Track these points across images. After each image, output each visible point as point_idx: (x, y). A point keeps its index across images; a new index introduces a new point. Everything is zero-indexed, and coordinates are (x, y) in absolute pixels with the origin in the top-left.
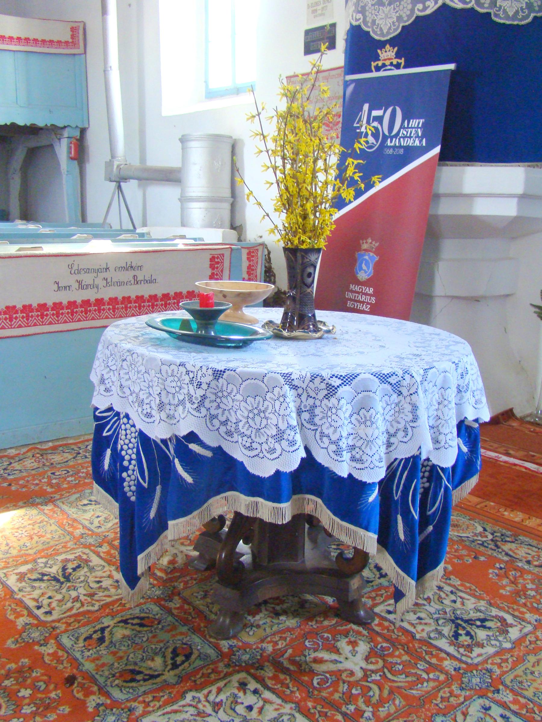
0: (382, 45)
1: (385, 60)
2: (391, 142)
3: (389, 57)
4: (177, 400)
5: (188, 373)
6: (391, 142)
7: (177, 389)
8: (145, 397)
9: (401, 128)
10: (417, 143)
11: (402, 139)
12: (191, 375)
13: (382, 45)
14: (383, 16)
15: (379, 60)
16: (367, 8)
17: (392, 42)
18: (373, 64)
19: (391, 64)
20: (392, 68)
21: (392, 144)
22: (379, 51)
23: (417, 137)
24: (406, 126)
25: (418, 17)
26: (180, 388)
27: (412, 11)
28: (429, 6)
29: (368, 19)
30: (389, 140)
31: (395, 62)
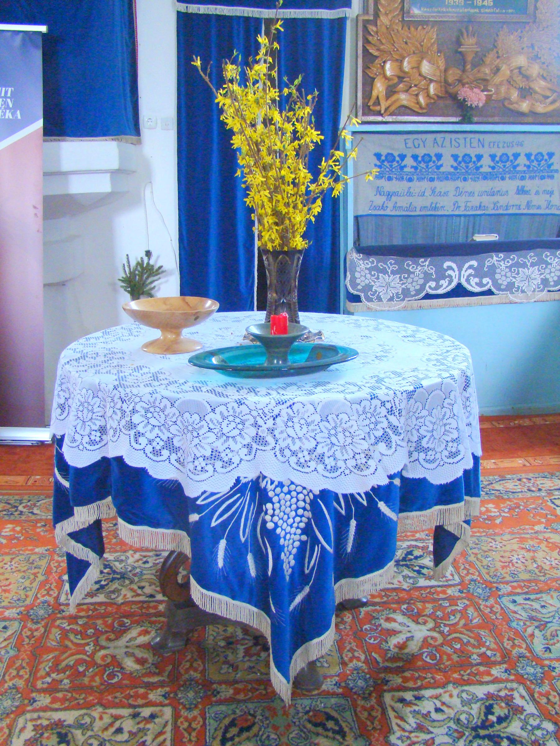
4: (373, 438)
5: (383, 404)
7: (372, 426)
8: (325, 450)
10: (9, 115)
12: (388, 405)
26: (376, 424)
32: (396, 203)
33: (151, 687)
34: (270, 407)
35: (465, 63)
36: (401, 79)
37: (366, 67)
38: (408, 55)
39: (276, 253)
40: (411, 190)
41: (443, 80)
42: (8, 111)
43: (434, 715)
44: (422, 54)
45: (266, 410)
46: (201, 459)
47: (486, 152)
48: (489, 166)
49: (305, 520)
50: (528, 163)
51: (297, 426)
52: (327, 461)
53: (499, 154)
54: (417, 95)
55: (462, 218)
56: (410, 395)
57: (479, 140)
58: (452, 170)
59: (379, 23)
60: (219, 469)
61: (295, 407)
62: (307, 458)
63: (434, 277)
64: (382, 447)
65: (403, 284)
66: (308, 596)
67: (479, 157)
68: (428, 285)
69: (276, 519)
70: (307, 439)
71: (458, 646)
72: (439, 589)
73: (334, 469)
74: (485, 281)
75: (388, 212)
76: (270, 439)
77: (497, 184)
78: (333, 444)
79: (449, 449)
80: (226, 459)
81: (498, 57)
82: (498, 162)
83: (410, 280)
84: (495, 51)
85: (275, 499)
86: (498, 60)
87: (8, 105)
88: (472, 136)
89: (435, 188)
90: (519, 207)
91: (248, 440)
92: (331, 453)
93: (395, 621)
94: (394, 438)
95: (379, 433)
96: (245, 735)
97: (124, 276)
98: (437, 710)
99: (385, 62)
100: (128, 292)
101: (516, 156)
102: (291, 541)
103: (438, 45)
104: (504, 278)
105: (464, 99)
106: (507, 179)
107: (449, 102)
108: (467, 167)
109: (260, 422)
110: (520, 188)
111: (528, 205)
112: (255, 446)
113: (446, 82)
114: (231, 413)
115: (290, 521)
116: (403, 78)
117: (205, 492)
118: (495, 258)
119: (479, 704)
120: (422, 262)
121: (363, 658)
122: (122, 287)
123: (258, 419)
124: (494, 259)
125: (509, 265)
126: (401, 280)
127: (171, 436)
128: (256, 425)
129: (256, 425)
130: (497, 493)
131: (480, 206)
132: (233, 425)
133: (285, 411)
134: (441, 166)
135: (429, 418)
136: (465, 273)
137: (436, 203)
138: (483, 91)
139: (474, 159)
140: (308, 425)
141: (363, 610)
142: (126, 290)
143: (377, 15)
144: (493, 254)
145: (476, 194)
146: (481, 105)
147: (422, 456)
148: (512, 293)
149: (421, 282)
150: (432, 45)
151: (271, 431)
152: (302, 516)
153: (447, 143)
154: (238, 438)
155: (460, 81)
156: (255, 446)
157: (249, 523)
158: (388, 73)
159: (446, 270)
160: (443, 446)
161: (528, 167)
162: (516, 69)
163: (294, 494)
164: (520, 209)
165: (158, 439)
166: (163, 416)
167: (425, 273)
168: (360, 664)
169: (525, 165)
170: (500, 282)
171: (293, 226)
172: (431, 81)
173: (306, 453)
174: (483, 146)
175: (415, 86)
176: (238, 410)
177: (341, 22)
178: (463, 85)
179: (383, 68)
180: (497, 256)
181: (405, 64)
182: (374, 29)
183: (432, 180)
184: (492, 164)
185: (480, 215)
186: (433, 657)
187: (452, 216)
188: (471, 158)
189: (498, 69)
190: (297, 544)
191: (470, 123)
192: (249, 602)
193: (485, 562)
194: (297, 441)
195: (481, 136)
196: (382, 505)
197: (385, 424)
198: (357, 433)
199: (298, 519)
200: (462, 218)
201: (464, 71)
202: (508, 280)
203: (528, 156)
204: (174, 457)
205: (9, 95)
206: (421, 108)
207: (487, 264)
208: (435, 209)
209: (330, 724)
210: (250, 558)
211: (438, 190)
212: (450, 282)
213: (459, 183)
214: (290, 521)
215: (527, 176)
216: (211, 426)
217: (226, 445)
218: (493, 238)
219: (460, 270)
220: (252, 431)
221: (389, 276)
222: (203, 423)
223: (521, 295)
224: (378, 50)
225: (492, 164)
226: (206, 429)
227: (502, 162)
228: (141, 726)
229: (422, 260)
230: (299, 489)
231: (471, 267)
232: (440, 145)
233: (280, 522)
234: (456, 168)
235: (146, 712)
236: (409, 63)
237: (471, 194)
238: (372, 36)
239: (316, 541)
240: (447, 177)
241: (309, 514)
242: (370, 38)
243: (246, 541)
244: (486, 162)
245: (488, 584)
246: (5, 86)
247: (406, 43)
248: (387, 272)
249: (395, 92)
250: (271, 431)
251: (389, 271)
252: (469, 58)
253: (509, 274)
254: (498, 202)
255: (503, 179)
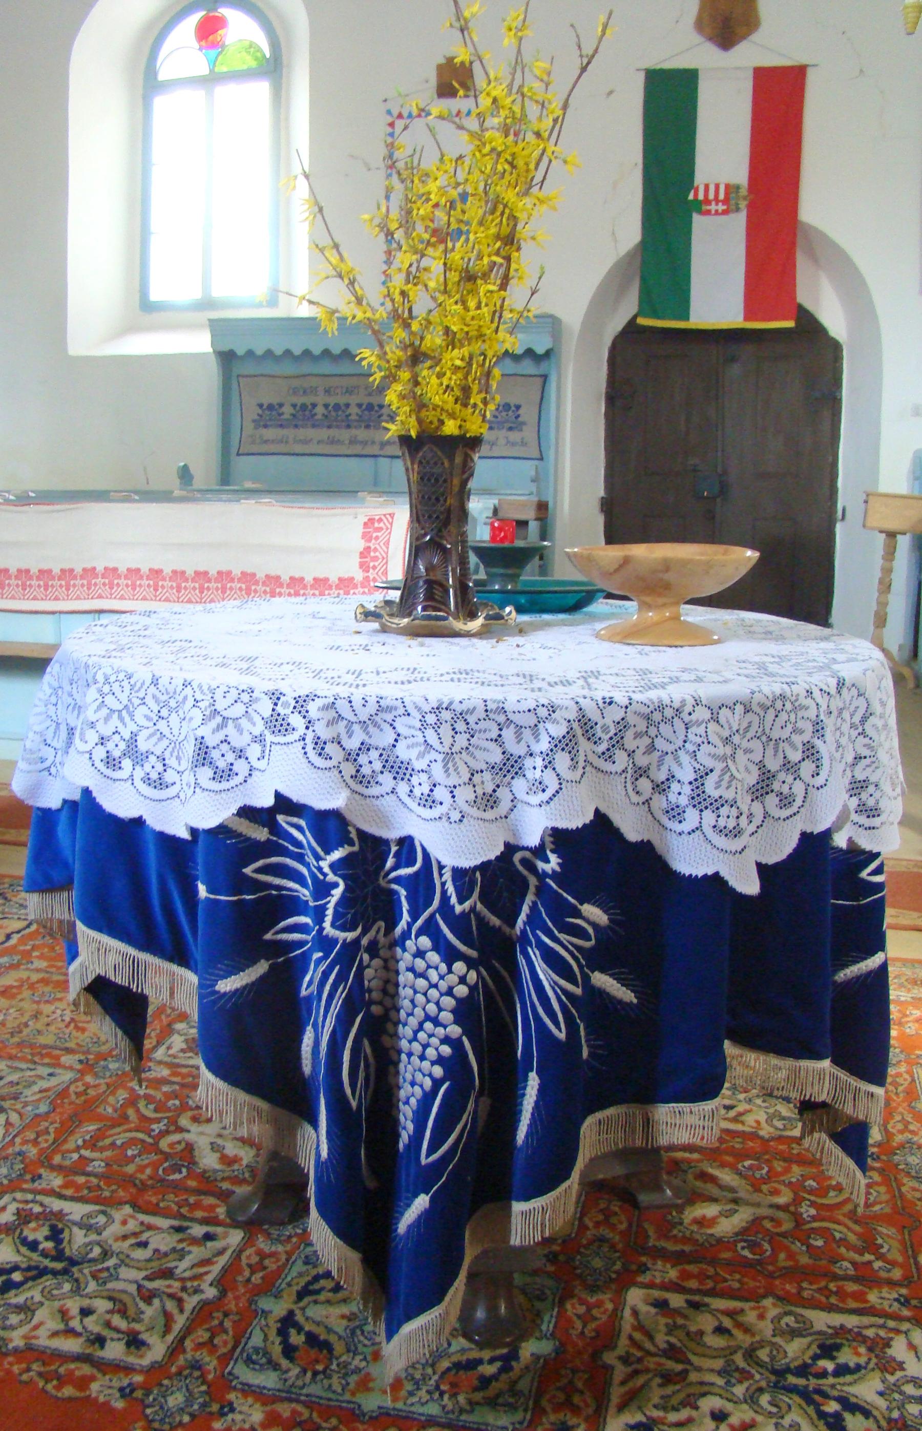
70: (376, 725)
76: (297, 721)
112: (269, 738)
127: (135, 728)
147: (709, 817)
156: (269, 738)
166: (127, 688)
194: (356, 727)
217: (221, 736)
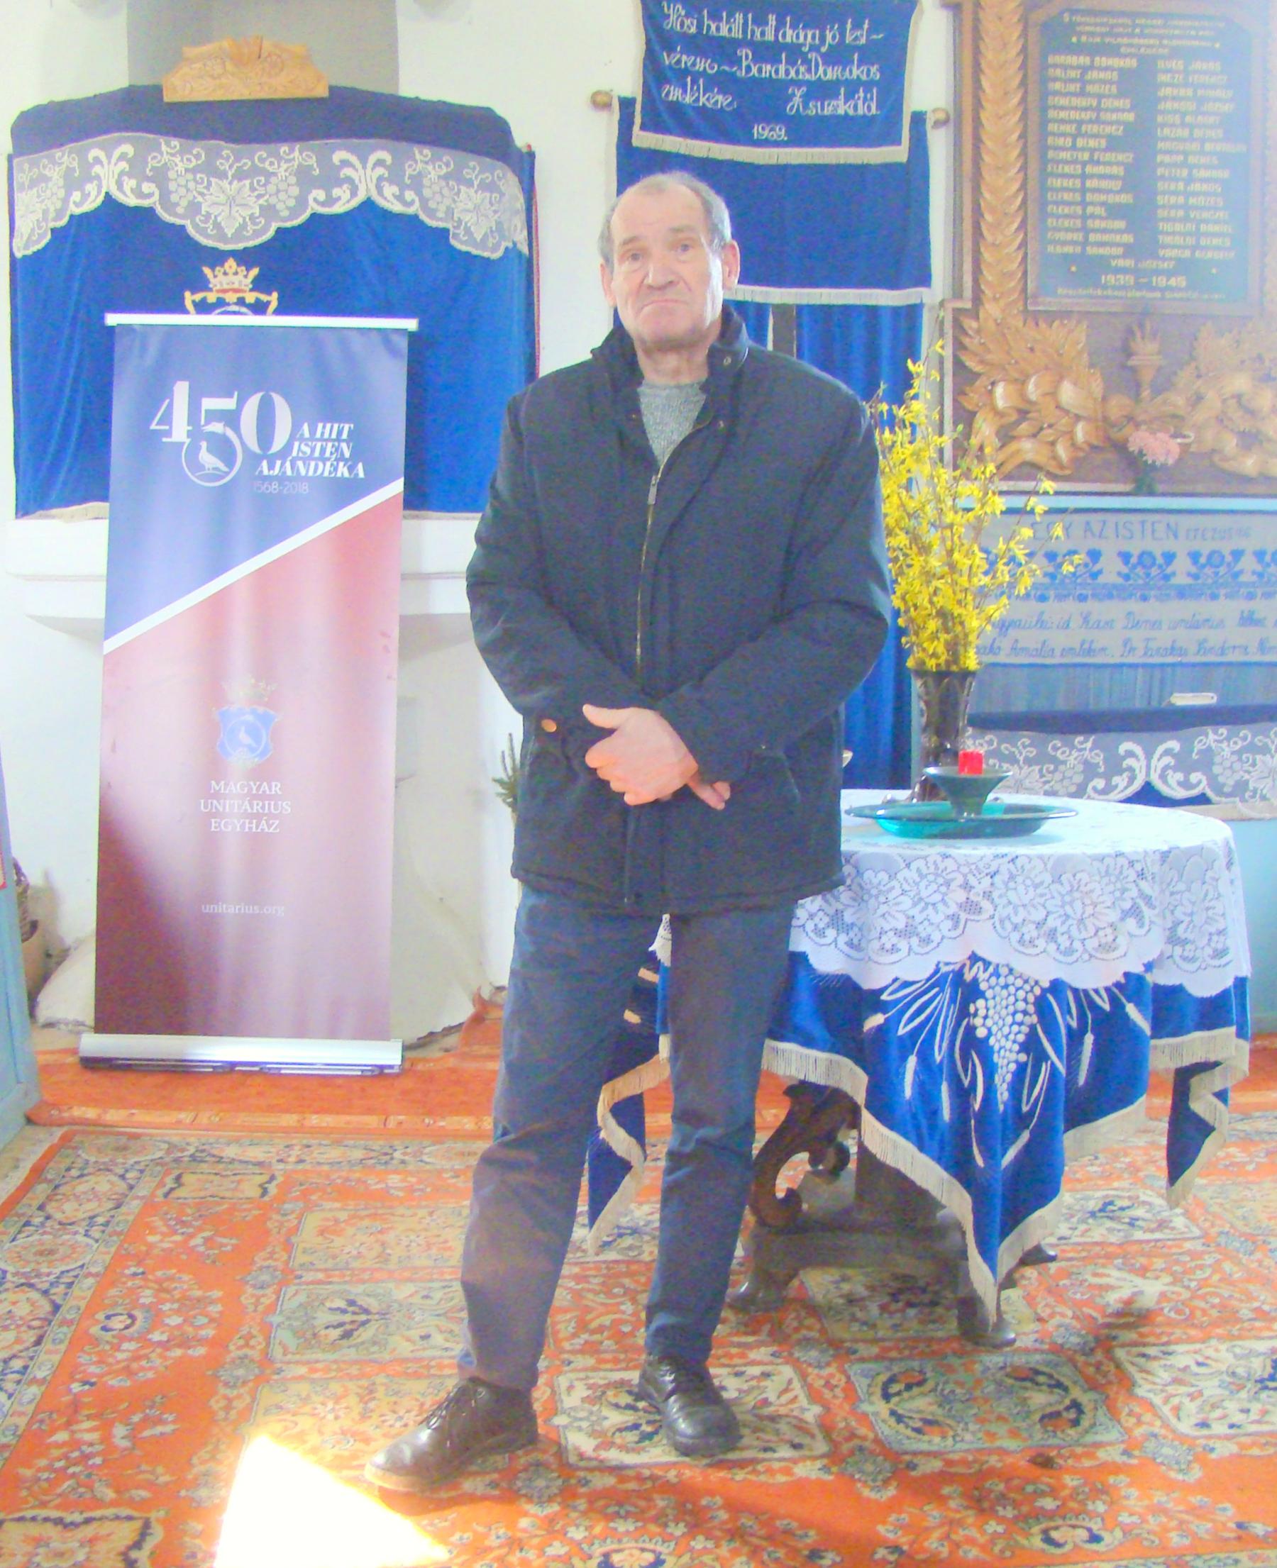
0: (217, 258)
1: (225, 291)
2: (271, 467)
3: (236, 286)
5: (1131, 864)
6: (271, 467)
7: (1117, 894)
9: (292, 438)
10: (343, 471)
11: (300, 464)
12: (1138, 867)
13: (217, 258)
14: (222, 198)
15: (210, 290)
16: (172, 175)
17: (245, 258)
18: (189, 298)
19: (241, 302)
20: (244, 310)
21: (276, 471)
22: (207, 271)
23: (341, 458)
24: (307, 435)
25: (314, 216)
26: (1123, 891)
27: (302, 201)
28: (339, 198)
29: (174, 198)
30: (265, 464)
31: (251, 298)
32: (1016, 641)
33: (749, 1346)
34: (985, 860)
35: (1138, 385)
36: (1023, 414)
37: (959, 392)
38: (1037, 372)
39: (941, 675)
40: (1045, 617)
41: (1100, 416)
42: (341, 464)
43: (1195, 1368)
44: (1059, 372)
45: (981, 865)
46: (891, 934)
47: (1181, 548)
48: (1189, 575)
49: (1025, 1029)
50: (1259, 568)
51: (1021, 888)
52: (1061, 939)
53: (1205, 552)
54: (1053, 444)
55: (1140, 670)
56: (1165, 856)
57: (1168, 525)
58: (1120, 581)
59: (982, 315)
60: (916, 948)
61: (1018, 862)
62: (1035, 933)
63: (1102, 770)
64: (1131, 923)
65: (1046, 783)
66: (1027, 1149)
67: (1169, 557)
68: (1090, 786)
69: (989, 1022)
70: (1034, 906)
71: (1217, 1301)
72: (1169, 1243)
73: (1069, 951)
74: (1194, 777)
75: (1002, 658)
76: (986, 904)
77: (1204, 608)
78: (1067, 916)
79: (1213, 944)
80: (923, 935)
81: (1199, 376)
82: (1203, 566)
83: (1058, 776)
84: (1193, 364)
85: (989, 994)
86: (1199, 383)
87: (342, 453)
88: (1156, 517)
89: (1089, 614)
90: (1245, 649)
91: (953, 909)
92: (1064, 929)
93: (1108, 1276)
94: (1147, 912)
95: (1127, 905)
96: (916, 1390)
97: (501, 775)
98: (1199, 1364)
99: (993, 384)
100: (510, 805)
101: (1237, 555)
102: (1005, 1061)
103: (1089, 354)
104: (1228, 773)
105: (1141, 452)
106: (1222, 598)
107: (1110, 456)
108: (1148, 575)
109: (973, 881)
110: (1245, 615)
111: (1263, 647)
112: (963, 916)
113: (1105, 419)
114: (932, 869)
115: (1006, 1030)
116: (1027, 412)
117: (895, 980)
118: (1211, 736)
119: (1261, 1358)
120: (1081, 743)
121: (1070, 1313)
122: (499, 795)
123: (970, 877)
124: (1211, 737)
125: (1237, 747)
126: (1042, 776)
128: (966, 886)
129: (966, 886)
130: (1242, 1135)
131: (1173, 648)
132: (934, 887)
133: (1005, 867)
134: (1100, 572)
135: (1187, 895)
136: (1158, 763)
137: (1092, 642)
138: (1174, 436)
139: (1160, 561)
140: (1036, 886)
141: (1053, 1266)
142: (504, 801)
143: (977, 299)
144: (1209, 730)
145: (1165, 626)
146: (1170, 462)
147: (1178, 950)
148: (1243, 800)
149: (1078, 779)
150: (1080, 353)
151: (987, 895)
152: (1020, 1024)
153: (1109, 531)
154: (940, 906)
155: (1130, 419)
156: (963, 916)
157: (947, 1035)
158: (1000, 403)
159: (1124, 758)
160: (1205, 941)
161: (1260, 575)
162: (1233, 397)
163: (1012, 989)
164: (1247, 654)
165: (821, 914)
167: (1086, 763)
168: (1067, 1321)
169: (1254, 573)
170: (1221, 779)
171: (966, 635)
172: (1078, 418)
173: (1032, 927)
174: (1176, 536)
175: (1050, 426)
176: (941, 866)
177: (912, 314)
178: (1137, 426)
179: (990, 393)
180: (1215, 733)
181: (1031, 387)
182: (974, 325)
183: (1082, 598)
184: (1194, 570)
185: (1173, 665)
186: (1178, 1312)
187: (1121, 665)
188: (1154, 559)
189: (1199, 398)
190: (1013, 1067)
191: (1151, 493)
192: (939, 1160)
193: (1239, 1212)
194: (1021, 909)
195: (1172, 519)
196: (1131, 1010)
197: (1134, 893)
198: (1101, 899)
199: (1015, 1028)
200: (1140, 670)
201: (1137, 398)
202: (1237, 777)
203: (1260, 555)
204: (843, 938)
205: (345, 436)
206: (1062, 467)
207: (1197, 746)
208: (1090, 652)
209: (1041, 1379)
210: (944, 1088)
211: (1093, 618)
212: (1132, 780)
213: (1134, 605)
214: (1006, 1030)
215: (1259, 592)
216: (906, 887)
217: (924, 915)
218: (1206, 699)
219: (1149, 756)
220: (961, 896)
221: (1021, 768)
222: (894, 883)
223: (1258, 803)
224: (982, 362)
225: (1194, 570)
226: (897, 891)
227: (1212, 566)
228: (754, 1383)
229: (1081, 738)
230: (1019, 982)
231: (1167, 752)
232: (1097, 533)
233: (994, 1029)
234: (1127, 577)
235: (755, 1371)
236: (1037, 386)
237: (1155, 625)
238: (971, 337)
239: (1041, 1056)
240: (1109, 593)
241: (1035, 1019)
242: (966, 341)
243: (941, 1062)
244: (1182, 565)
245: (1250, 1237)
246: (340, 422)
247: (1032, 350)
248: (1017, 762)
249: (1013, 438)
250: (987, 895)
251: (1021, 759)
252: (1147, 377)
253: (1237, 766)
254: (1205, 640)
255: (1214, 597)
